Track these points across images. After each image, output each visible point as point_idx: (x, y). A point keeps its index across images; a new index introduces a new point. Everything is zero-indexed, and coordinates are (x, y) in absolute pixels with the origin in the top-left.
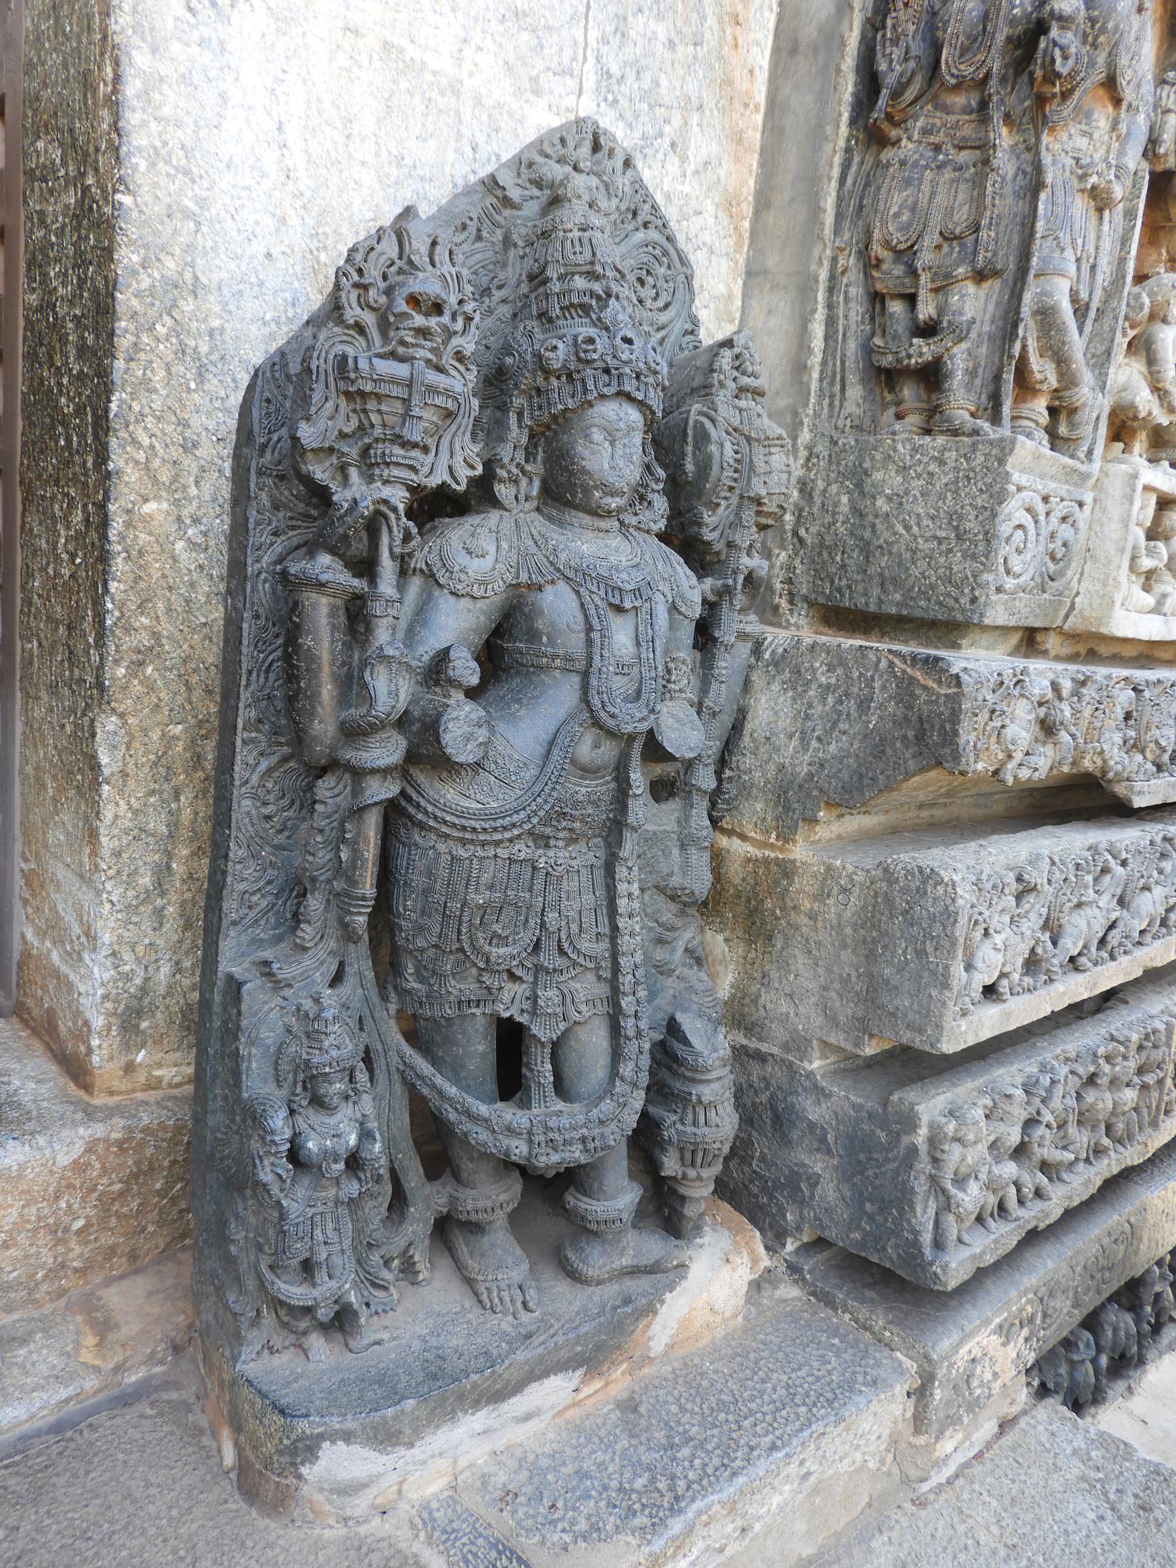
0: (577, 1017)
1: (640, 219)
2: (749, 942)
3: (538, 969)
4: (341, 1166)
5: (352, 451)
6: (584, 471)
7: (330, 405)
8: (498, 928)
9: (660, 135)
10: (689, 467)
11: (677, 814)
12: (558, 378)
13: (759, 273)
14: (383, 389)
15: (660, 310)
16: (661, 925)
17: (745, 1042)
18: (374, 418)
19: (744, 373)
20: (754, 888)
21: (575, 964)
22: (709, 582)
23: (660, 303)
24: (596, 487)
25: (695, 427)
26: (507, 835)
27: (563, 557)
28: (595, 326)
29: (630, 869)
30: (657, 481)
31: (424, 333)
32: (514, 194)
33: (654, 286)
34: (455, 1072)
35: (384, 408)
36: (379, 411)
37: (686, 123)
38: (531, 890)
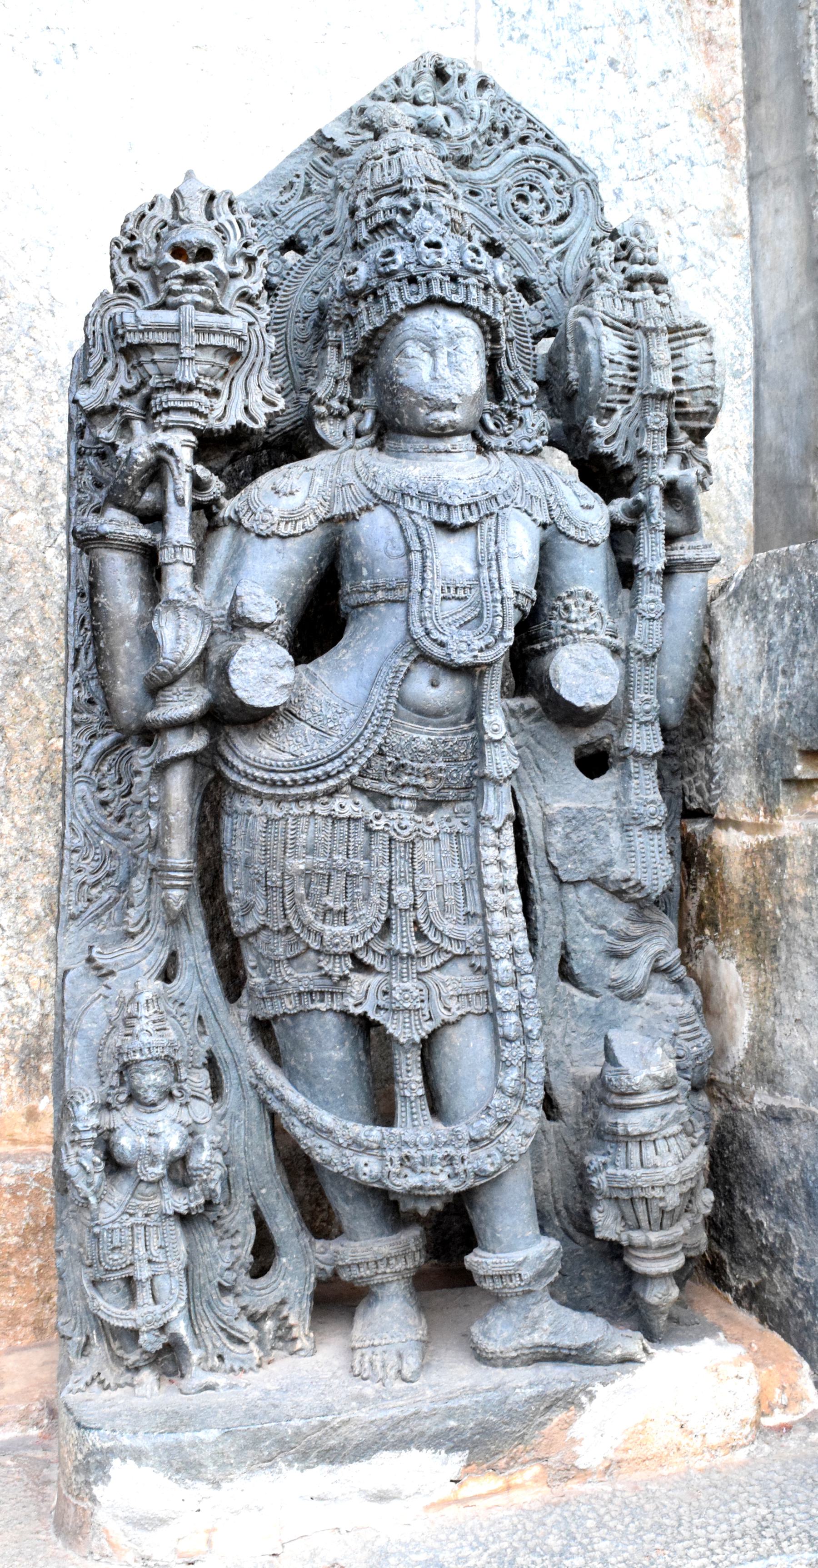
0: (445, 1015)
1: (513, 137)
2: (757, 962)
3: (394, 955)
4: (159, 1170)
5: (132, 406)
6: (403, 388)
7: (109, 367)
8: (328, 901)
9: (593, 57)
10: (573, 375)
11: (614, 789)
12: (365, 299)
13: (761, 173)
14: (151, 338)
15: (555, 223)
16: (611, 933)
17: (770, 1101)
18: (150, 368)
19: (634, 262)
20: (754, 888)
21: (440, 950)
22: (619, 504)
23: (553, 216)
24: (419, 404)
25: (574, 330)
26: (322, 787)
27: (382, 481)
28: (403, 239)
29: (498, 831)
30: (526, 394)
31: (192, 279)
32: (343, 142)
33: (542, 201)
34: (310, 1085)
35: (156, 357)
36: (154, 362)
37: (627, 38)
38: (367, 857)
